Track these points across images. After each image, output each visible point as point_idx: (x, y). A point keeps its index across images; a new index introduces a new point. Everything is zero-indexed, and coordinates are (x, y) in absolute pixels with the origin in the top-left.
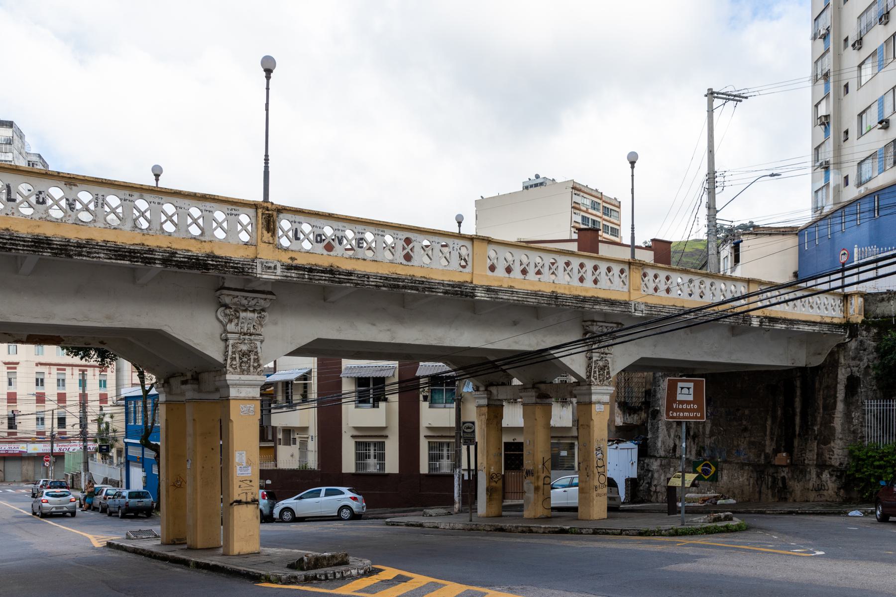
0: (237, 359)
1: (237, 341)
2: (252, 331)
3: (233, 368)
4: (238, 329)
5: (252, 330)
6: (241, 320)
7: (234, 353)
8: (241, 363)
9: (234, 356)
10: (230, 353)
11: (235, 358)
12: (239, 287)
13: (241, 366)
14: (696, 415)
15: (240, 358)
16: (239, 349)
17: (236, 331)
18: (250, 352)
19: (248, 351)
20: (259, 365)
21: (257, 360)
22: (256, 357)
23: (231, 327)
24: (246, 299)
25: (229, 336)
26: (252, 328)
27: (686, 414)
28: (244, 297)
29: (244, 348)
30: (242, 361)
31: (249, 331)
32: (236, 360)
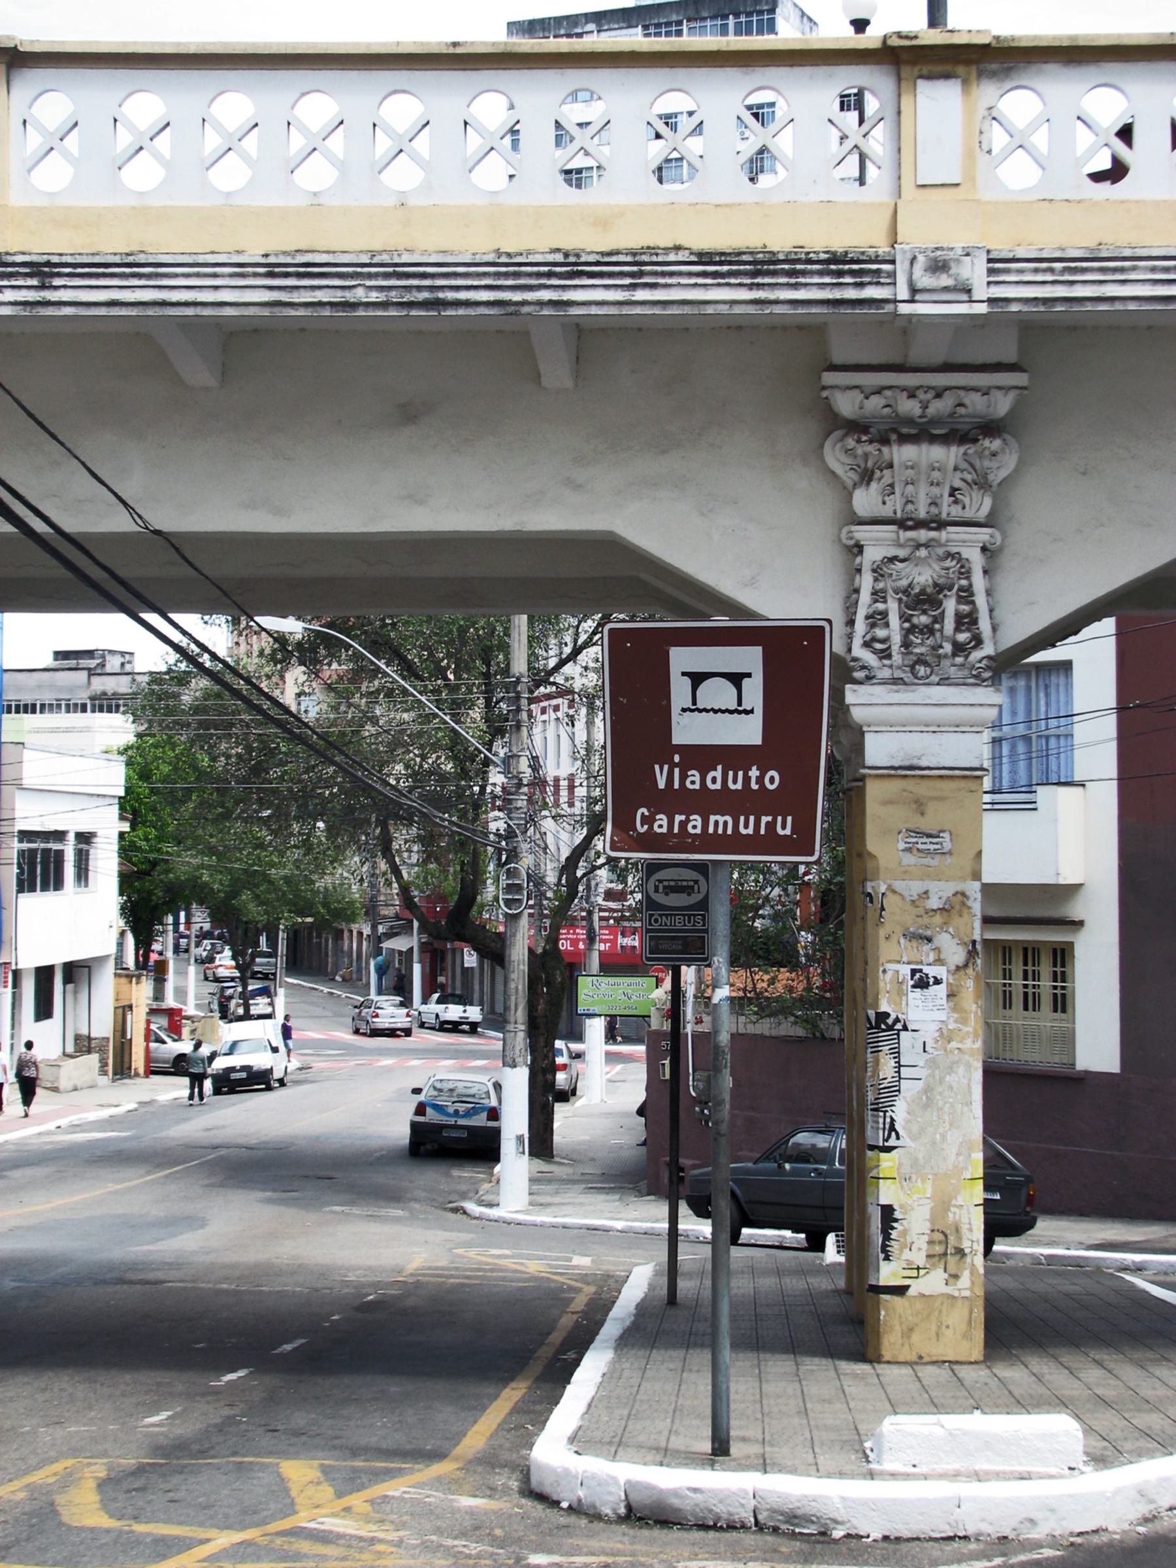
0: (894, 620)
1: (892, 552)
2: (945, 510)
3: (875, 652)
4: (894, 506)
5: (947, 509)
6: (900, 475)
7: (878, 595)
8: (909, 632)
9: (881, 606)
10: (865, 597)
11: (884, 614)
12: (874, 360)
13: (906, 644)
14: (771, 826)
15: (904, 618)
16: (904, 583)
17: (886, 511)
18: (940, 588)
19: (936, 585)
20: (978, 641)
21: (966, 621)
22: (965, 608)
23: (866, 501)
24: (912, 396)
25: (862, 533)
26: (947, 500)
27: (720, 822)
28: (903, 389)
29: (923, 576)
30: (914, 626)
31: (934, 510)
32: (887, 625)
